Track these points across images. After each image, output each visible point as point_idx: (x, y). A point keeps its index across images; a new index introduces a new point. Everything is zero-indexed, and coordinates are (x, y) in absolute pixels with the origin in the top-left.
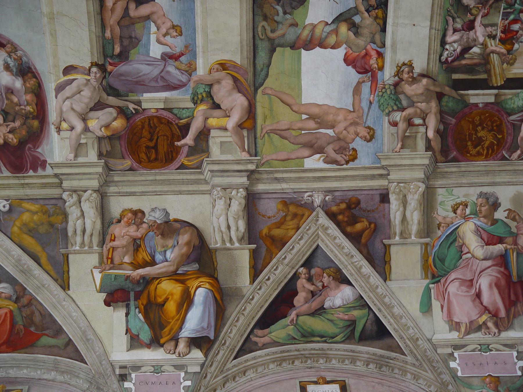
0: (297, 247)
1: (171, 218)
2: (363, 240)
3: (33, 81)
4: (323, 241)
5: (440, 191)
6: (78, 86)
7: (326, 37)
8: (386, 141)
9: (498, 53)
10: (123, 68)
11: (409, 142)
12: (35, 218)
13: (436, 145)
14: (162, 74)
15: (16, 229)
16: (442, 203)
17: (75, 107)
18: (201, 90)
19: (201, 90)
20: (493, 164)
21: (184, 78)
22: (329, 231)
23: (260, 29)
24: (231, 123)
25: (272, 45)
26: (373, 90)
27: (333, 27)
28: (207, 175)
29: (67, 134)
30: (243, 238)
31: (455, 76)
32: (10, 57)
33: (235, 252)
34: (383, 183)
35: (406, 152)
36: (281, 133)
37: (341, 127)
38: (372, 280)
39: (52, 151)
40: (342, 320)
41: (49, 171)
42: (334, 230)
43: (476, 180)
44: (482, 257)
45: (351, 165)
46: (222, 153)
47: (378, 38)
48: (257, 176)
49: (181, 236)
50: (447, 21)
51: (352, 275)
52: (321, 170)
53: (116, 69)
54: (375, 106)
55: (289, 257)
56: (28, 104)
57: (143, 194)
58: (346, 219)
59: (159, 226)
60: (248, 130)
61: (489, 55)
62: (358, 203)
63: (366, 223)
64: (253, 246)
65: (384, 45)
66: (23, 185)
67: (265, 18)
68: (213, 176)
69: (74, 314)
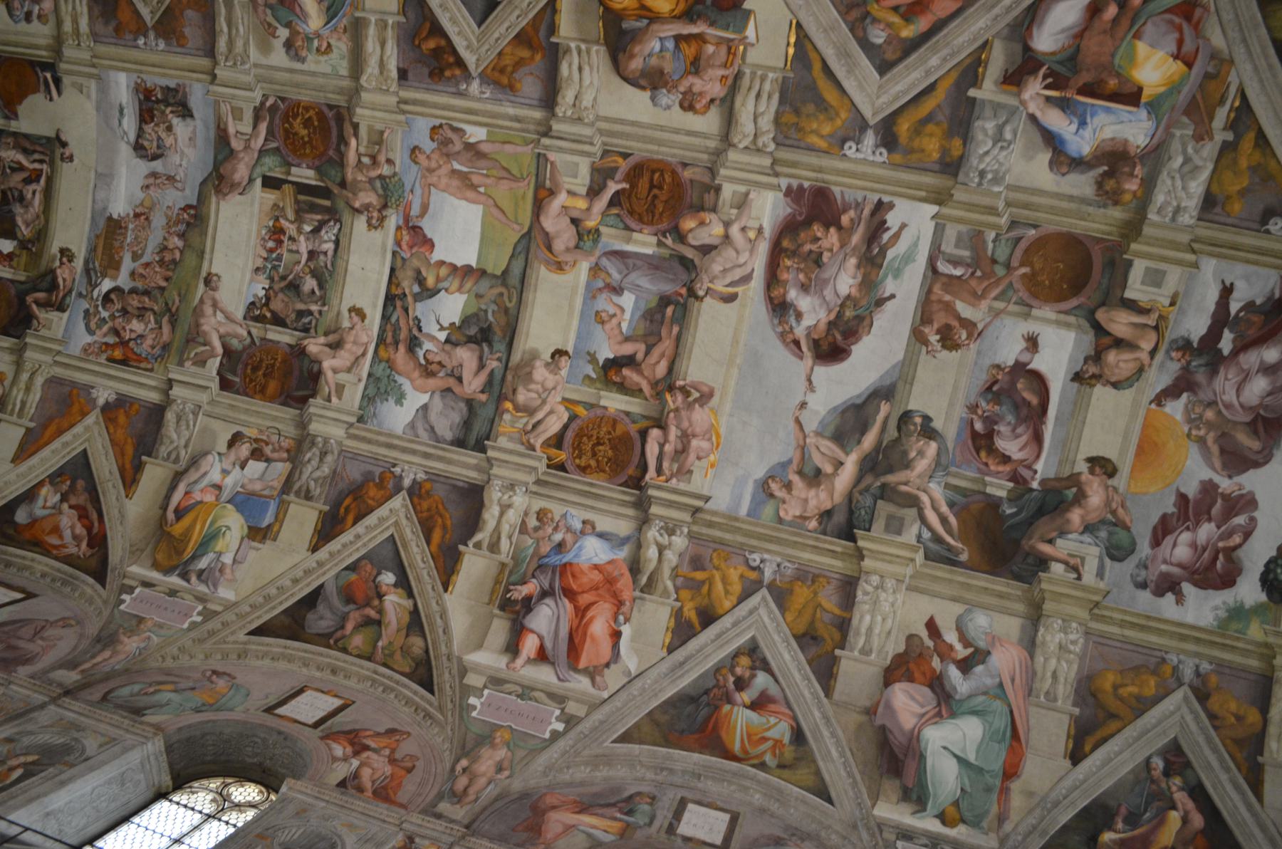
0: (503, 29)
1: (648, 94)
2: (428, 25)
3: (775, 293)
4: (473, 32)
5: (344, 72)
6: (724, 278)
8: (399, 144)
9: (287, 219)
10: (668, 288)
12: (815, 126)
13: (348, 129)
14: (626, 272)
15: (843, 115)
16: (342, 58)
17: (733, 254)
19: (588, 244)
20: (293, 95)
21: (605, 262)
22: (465, 43)
23: (514, 300)
24: (561, 199)
27: (441, 285)
28: (598, 140)
30: (565, 53)
31: (327, 203)
32: (791, 328)
34: (405, 94)
35: (379, 127)
36: (509, 175)
37: (444, 170)
39: (775, 207)
41: (784, 182)
42: (460, 44)
43: (309, 79)
45: (437, 122)
46: (577, 165)
48: (542, 129)
49: (640, 67)
52: (469, 122)
53: (677, 288)
54: (408, 188)
56: (788, 268)
57: (677, 131)
59: (665, 85)
60: (544, 187)
62: (431, 75)
63: (424, 47)
64: (553, 40)
65: (394, 253)
66: (820, 170)
67: (506, 311)
68: (591, 138)
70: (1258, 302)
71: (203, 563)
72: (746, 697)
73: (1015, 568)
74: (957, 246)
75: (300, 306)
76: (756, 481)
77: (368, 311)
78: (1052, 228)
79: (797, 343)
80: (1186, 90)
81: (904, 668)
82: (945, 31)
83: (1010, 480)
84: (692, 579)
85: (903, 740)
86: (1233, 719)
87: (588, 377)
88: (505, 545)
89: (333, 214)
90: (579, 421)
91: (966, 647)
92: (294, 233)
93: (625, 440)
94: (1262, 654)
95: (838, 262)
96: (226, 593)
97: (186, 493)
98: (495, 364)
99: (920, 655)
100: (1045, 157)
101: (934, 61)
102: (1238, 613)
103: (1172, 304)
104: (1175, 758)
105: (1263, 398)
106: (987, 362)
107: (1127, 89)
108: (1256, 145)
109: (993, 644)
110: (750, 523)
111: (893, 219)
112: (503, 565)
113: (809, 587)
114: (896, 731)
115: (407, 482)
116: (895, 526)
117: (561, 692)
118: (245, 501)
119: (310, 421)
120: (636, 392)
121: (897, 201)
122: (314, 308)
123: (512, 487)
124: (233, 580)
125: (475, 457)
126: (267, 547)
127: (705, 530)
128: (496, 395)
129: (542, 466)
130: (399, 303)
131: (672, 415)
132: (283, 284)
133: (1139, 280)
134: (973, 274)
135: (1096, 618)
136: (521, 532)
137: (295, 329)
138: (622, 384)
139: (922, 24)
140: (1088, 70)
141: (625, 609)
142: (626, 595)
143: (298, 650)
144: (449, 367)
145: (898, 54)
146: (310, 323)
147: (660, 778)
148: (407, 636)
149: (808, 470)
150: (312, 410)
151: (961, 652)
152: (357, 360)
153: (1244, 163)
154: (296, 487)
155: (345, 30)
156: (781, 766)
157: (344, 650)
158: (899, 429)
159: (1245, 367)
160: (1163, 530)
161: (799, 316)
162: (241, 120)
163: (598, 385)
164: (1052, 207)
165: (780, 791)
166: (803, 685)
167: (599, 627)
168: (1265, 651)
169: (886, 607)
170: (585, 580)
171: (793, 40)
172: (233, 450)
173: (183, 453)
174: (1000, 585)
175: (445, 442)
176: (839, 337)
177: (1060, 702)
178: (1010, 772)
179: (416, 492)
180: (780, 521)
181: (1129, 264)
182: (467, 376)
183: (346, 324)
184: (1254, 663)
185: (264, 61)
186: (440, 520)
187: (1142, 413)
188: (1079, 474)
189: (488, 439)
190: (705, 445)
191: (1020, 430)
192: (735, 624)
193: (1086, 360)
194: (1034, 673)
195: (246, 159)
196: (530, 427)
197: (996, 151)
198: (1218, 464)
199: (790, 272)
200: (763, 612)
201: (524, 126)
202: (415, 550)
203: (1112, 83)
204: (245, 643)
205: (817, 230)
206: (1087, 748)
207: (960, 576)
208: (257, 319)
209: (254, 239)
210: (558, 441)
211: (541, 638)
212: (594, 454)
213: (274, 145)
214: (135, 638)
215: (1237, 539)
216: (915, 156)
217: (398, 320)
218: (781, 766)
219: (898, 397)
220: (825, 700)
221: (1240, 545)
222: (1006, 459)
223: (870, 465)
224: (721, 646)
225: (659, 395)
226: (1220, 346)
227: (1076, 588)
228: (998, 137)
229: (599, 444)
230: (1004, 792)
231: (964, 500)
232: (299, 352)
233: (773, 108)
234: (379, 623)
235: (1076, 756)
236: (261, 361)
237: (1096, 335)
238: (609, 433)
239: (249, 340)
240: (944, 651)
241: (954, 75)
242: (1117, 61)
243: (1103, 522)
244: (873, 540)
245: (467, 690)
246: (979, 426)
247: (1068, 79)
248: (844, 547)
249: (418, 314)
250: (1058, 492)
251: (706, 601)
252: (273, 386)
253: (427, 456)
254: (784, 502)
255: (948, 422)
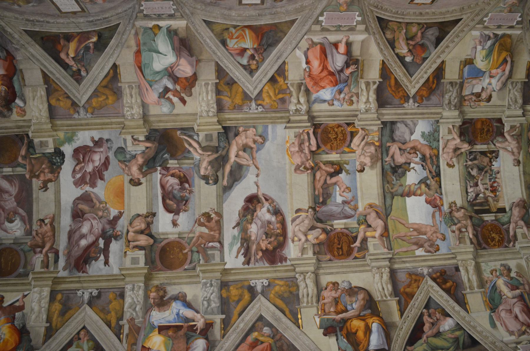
1: (353, 285)
2: (452, 292)
3: (280, 217)
4: (432, 293)
5: (482, 264)
7: (416, 191)
8: (451, 240)
9: (491, 197)
10: (324, 208)
11: (462, 240)
12: (282, 288)
13: (475, 241)
15: (272, 295)
16: (485, 270)
17: (301, 229)
18: (361, 218)
19: (361, 218)
20: (502, 250)
21: (353, 213)
22: (434, 288)
23: (386, 188)
24: (377, 234)
25: (392, 195)
26: (440, 216)
27: (418, 186)
28: (368, 262)
29: (296, 243)
30: (391, 294)
31: (476, 208)
32: (270, 205)
33: (389, 302)
35: (462, 245)
37: (429, 234)
38: (461, 313)
39: (290, 252)
40: (451, 338)
41: (289, 263)
42: (436, 287)
44: (511, 297)
45: (437, 253)
46: (375, 249)
47: (438, 190)
48: (393, 260)
49: (359, 296)
50: (466, 183)
51: (450, 311)
54: (443, 223)
55: (417, 303)
56: (278, 229)
57: (337, 273)
58: (441, 281)
60: (386, 237)
61: (487, 197)
62: (445, 272)
63: (451, 283)
65: (441, 194)
66: (275, 271)
67: (388, 182)
68: (371, 262)
69: (307, 342)
70: (94, 261)
71: (489, 43)
72: (249, 53)
73: (158, 134)
74: (214, 254)
75: (476, 162)
76: (268, 140)
77: (446, 167)
78: (179, 270)
79: (267, 200)
80: (142, 337)
81: (190, 82)
82: (240, 338)
83: (169, 167)
84: (283, 94)
85: (183, 53)
86: (60, 98)
87: (347, 164)
88: (363, 87)
89: (472, 204)
90: (346, 145)
91: (169, 97)
92: (487, 192)
93: (325, 143)
94: (56, 127)
95: (259, 236)
96: (476, 33)
97: (504, 71)
98: (387, 159)
99: (185, 89)
100: (189, 298)
101: (242, 325)
102: (69, 140)
103: (126, 252)
104: (77, 77)
105: (82, 225)
106: (190, 212)
107: (164, 332)
108: (110, 322)
109: (158, 101)
110: (266, 123)
111: (242, 259)
112: (362, 78)
113: (236, 104)
114: (186, 56)
115: (411, 101)
116: (209, 137)
117: (324, 33)
118: (478, 74)
119: (459, 115)
120: (326, 163)
121: (242, 266)
122: (470, 163)
123: (367, 111)
124: (474, 40)
125: (385, 119)
126: (463, 57)
127: (283, 115)
128: (384, 147)
129: (357, 123)
130: (434, 174)
131: (309, 158)
132: (486, 169)
133: (140, 258)
134: (205, 245)
135: (122, 123)
136: (358, 93)
137: (475, 152)
138: (333, 165)
139: (250, 339)
140: (181, 336)
141: (307, 74)
142: (308, 80)
143: (438, 18)
144: (406, 153)
145: (256, 325)
146: (470, 156)
147: (274, 10)
148: (394, 38)
149: (249, 150)
150: (459, 120)
151: (170, 95)
152: (445, 146)
153: (113, 314)
154: (458, 86)
155: (487, 282)
156: (227, 29)
157: (419, 24)
158: (217, 176)
159: (92, 235)
160: (106, 164)
161: (269, 211)
162: (522, 234)
163: (342, 162)
164: (181, 279)
165: (225, 19)
166: (228, 64)
167: (316, 64)
168: (56, 128)
169: (204, 104)
170: (327, 81)
171: (300, 321)
172: (489, 94)
173: (510, 87)
174: (162, 126)
175: (399, 122)
176: (250, 206)
177: (127, 86)
178: (138, 53)
179: (406, 98)
180: (254, 127)
181: (146, 264)
182: (398, 151)
183: (454, 160)
184: (59, 122)
185: (518, 261)
186: (393, 89)
187: (126, 207)
188: (143, 177)
189: (382, 128)
190: (292, 149)
191: (171, 188)
192: (261, 80)
193: (152, 222)
194: (139, 94)
195: (515, 218)
196: (366, 137)
197: (208, 295)
198: (92, 195)
199: (276, 227)
200: (251, 89)
201: (401, 260)
202: (400, 74)
203: (170, 333)
204: (462, 14)
205: (270, 247)
206: (111, 71)
207: (178, 125)
208: (493, 152)
209: (503, 185)
210: (353, 135)
211: (338, 53)
212: (336, 133)
213: (505, 227)
214: (510, 3)
215: (78, 168)
216: (239, 286)
217: (433, 167)
218: (227, 29)
219: (221, 189)
220: (217, 60)
221: (76, 166)
222: (173, 175)
223: (224, 159)
224: (264, 70)
225: (316, 164)
226: (103, 241)
227: (133, 133)
228: (209, 301)
229: (336, 138)
230: (138, 45)
231: (185, 155)
232: (471, 143)
233: (301, 291)
234: (407, 39)
235: (115, 67)
236: (487, 135)
237: (151, 233)
238: (332, 144)
239: (494, 142)
240: (176, 93)
241: (232, 322)
242: (171, 342)
243: (129, 161)
244: (216, 129)
245: (363, 22)
246: (187, 185)
247: (188, 331)
248: (226, 123)
249: (425, 172)
250: (149, 168)
251: (275, 87)
252: (479, 126)
253: (406, 114)
254: (255, 135)
255: (199, 184)
